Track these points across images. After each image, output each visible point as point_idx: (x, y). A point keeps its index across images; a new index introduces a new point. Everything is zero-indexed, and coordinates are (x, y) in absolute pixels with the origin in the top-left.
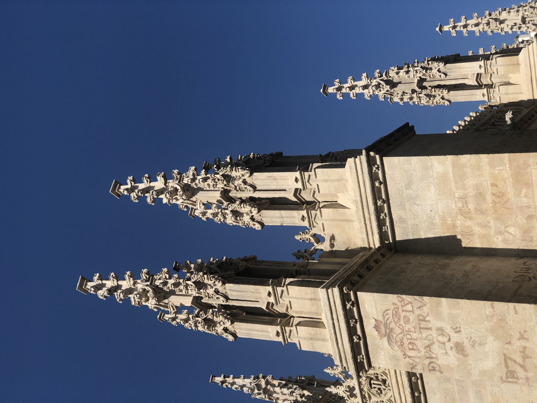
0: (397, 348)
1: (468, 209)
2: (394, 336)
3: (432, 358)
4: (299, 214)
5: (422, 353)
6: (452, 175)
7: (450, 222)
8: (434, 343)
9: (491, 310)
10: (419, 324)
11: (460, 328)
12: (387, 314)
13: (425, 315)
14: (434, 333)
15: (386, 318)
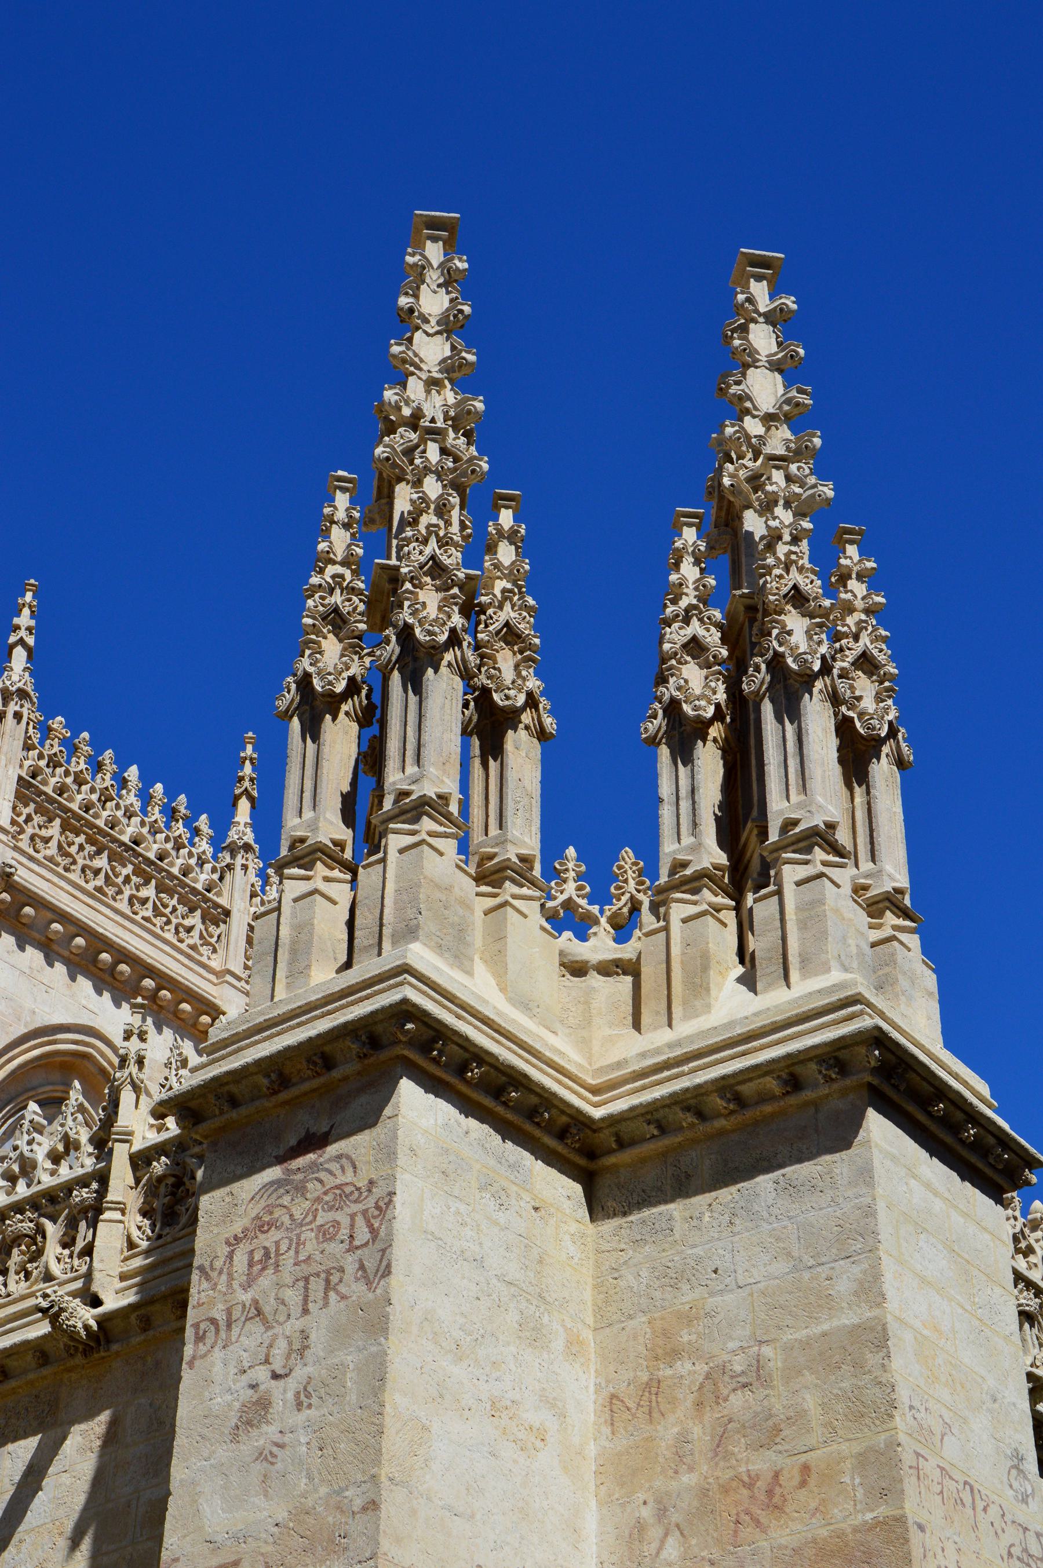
1: (725, 1392)
2: (286, 1200)
3: (229, 1326)
6: (826, 1327)
7: (686, 1338)
9: (358, 1503)
10: (318, 1275)
13: (342, 1288)
15: (334, 1166)
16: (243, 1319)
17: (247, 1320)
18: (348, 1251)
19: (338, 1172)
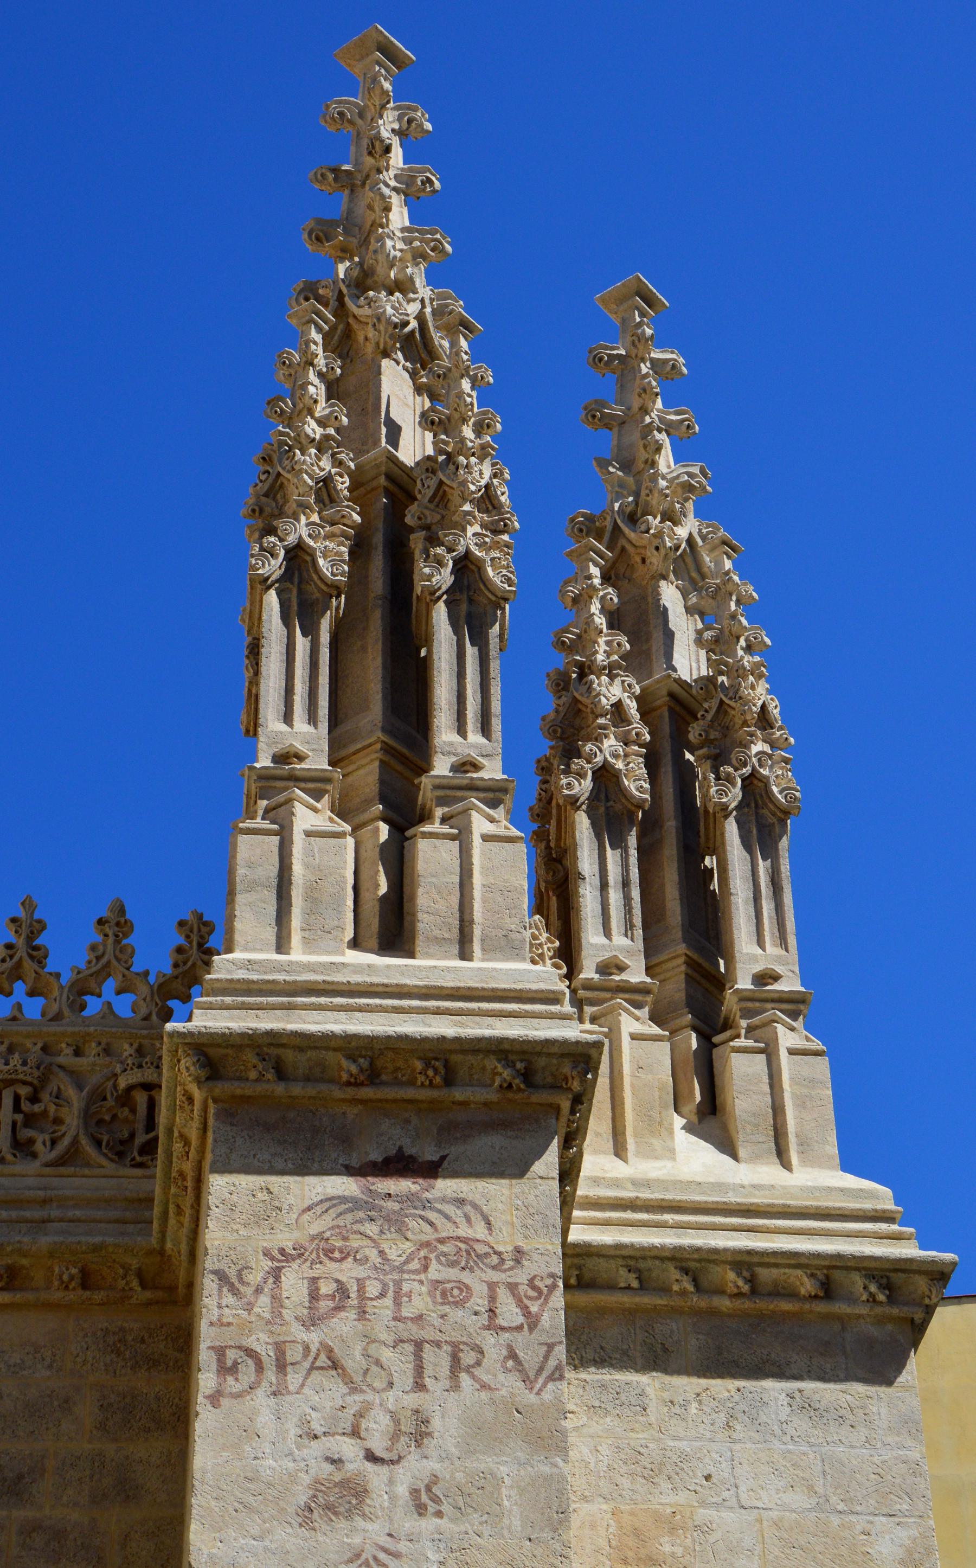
0: (315, 1229)
2: (371, 1229)
3: (282, 1366)
4: (629, 952)
5: (298, 1332)
8: (355, 1390)
10: (438, 1344)
11: (439, 1514)
12: (468, 1220)
14: (402, 1398)
15: (450, 1209)
16: (307, 1365)
17: (312, 1368)
18: (488, 1328)
19: (461, 1221)
